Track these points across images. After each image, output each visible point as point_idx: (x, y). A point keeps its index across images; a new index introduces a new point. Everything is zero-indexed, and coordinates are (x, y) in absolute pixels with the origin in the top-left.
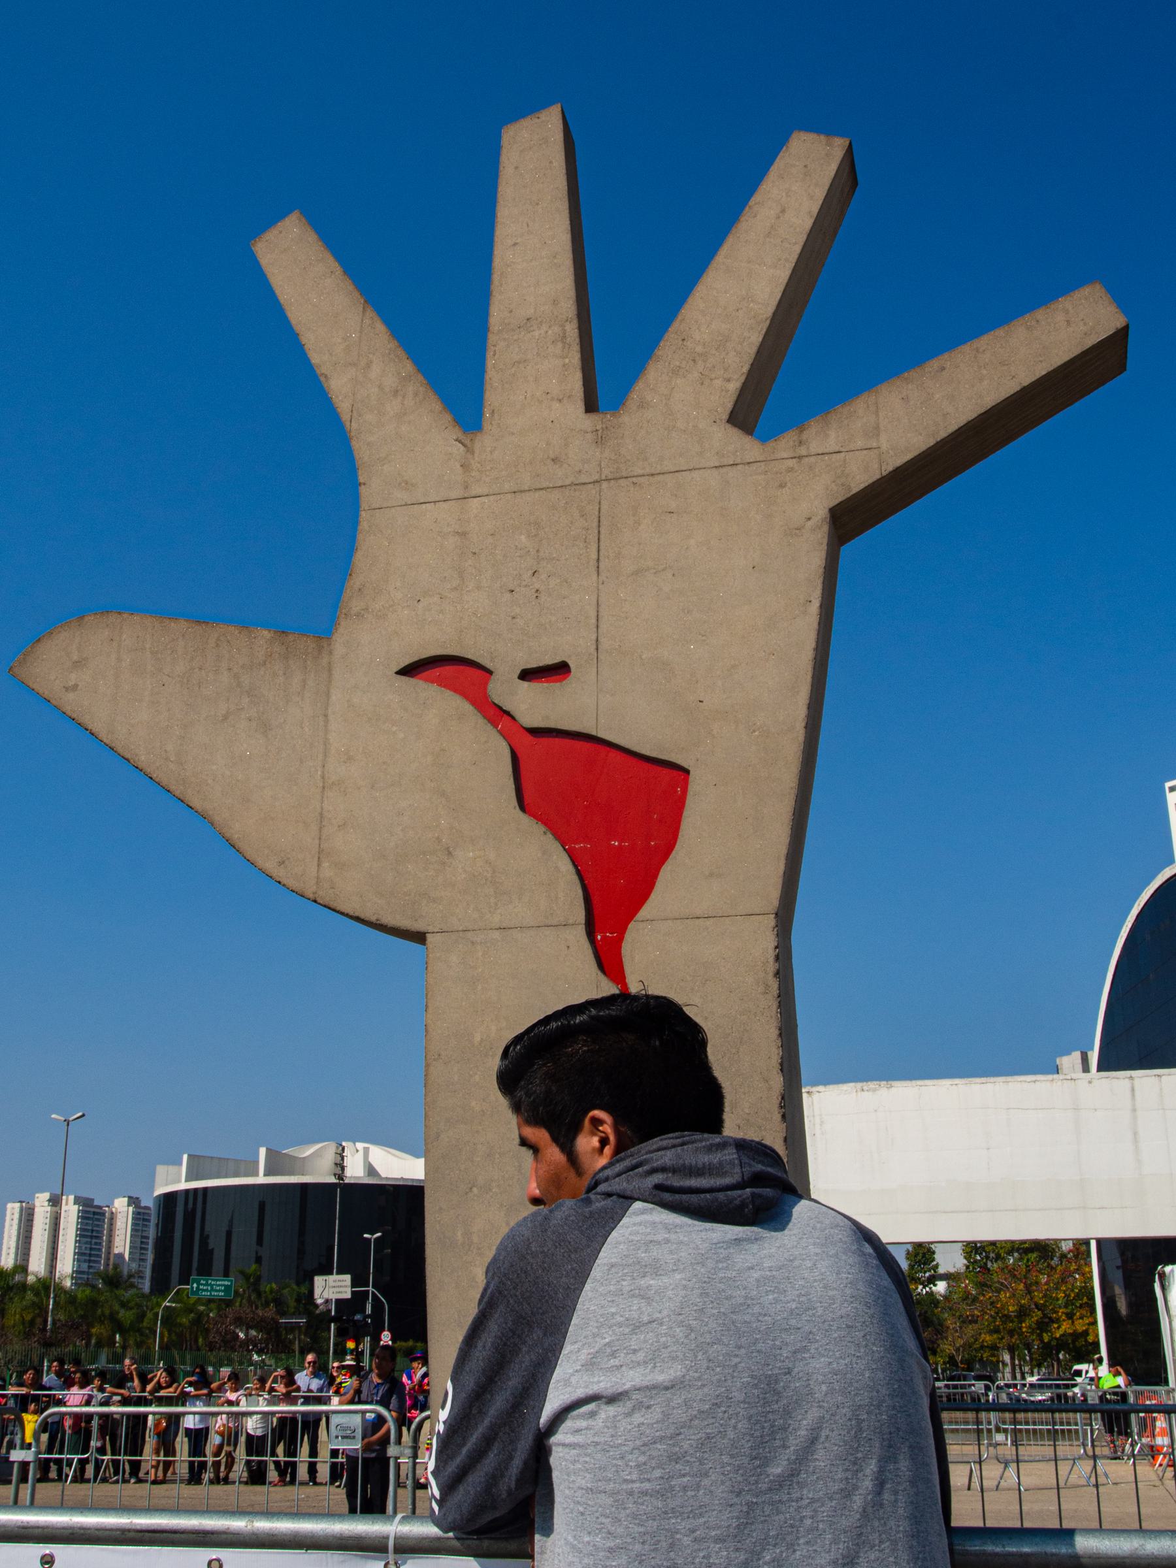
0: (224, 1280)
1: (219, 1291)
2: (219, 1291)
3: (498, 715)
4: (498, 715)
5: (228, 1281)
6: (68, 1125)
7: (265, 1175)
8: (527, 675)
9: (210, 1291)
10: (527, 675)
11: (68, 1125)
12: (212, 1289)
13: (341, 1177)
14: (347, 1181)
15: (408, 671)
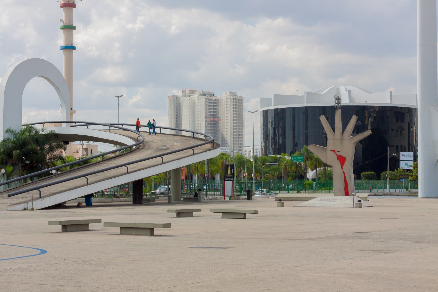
0: (301, 157)
1: (300, 160)
2: (300, 160)
3: (336, 154)
4: (336, 154)
5: (302, 157)
6: (253, 114)
7: (307, 103)
8: (337, 151)
9: (297, 160)
10: (337, 151)
11: (253, 114)
12: (298, 159)
13: (339, 103)
14: (342, 105)
15: (331, 150)
